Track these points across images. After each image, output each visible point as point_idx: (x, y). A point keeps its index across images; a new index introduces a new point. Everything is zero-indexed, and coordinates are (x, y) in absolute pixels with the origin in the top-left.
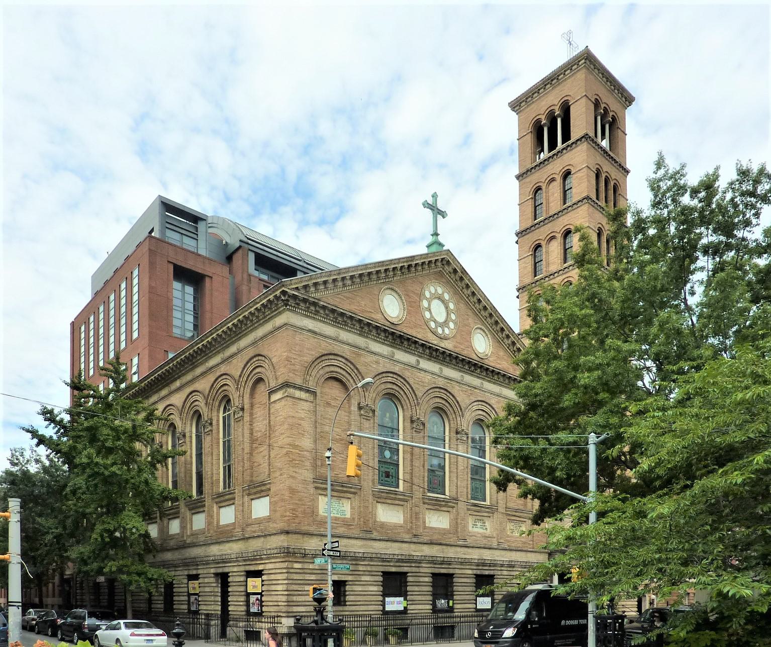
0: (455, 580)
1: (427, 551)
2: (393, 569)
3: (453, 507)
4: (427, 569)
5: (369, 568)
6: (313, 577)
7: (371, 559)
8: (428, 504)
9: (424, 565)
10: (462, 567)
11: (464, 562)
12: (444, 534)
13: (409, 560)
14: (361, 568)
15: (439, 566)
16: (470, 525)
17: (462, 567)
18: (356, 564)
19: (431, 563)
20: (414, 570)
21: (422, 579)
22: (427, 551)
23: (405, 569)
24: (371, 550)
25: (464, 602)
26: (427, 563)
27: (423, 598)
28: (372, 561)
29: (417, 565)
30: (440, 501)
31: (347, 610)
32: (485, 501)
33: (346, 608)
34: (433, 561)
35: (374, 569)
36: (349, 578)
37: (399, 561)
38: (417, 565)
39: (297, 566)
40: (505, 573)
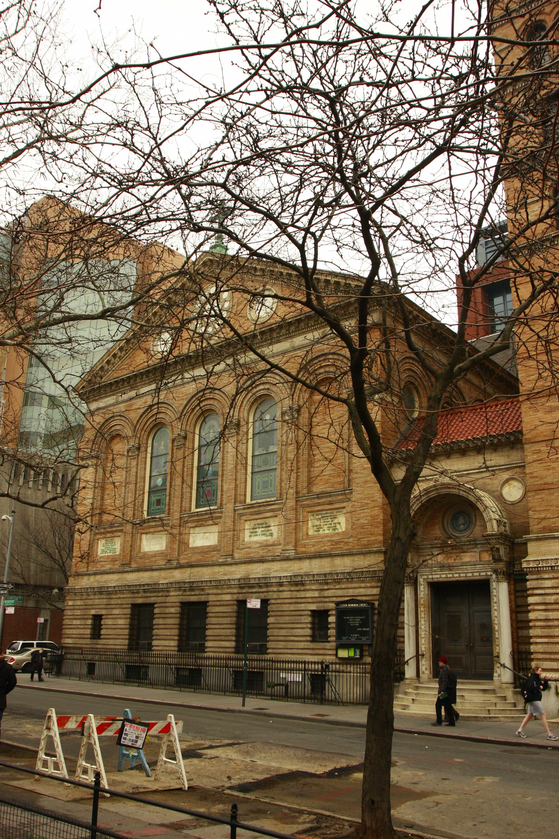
0: (209, 609)
1: (178, 575)
2: (140, 601)
3: (220, 517)
4: (175, 597)
5: (119, 601)
6: (78, 612)
7: (121, 592)
8: (190, 522)
9: (172, 594)
10: (219, 591)
11: (219, 584)
12: (206, 553)
13: (153, 588)
14: (113, 602)
15: (188, 593)
16: (247, 533)
17: (219, 591)
18: (267, 592)
19: (180, 590)
20: (160, 599)
21: (167, 610)
22: (178, 575)
23: (152, 600)
24: (125, 583)
25: (218, 638)
26: (176, 591)
27: (168, 632)
28: (123, 593)
29: (164, 594)
30: (202, 515)
31: (101, 643)
32: (196, 508)
33: (100, 641)
34: (180, 586)
35: (123, 601)
36: (103, 612)
37: (145, 591)
38: (164, 594)
39: (70, 603)
40: (286, 595)
